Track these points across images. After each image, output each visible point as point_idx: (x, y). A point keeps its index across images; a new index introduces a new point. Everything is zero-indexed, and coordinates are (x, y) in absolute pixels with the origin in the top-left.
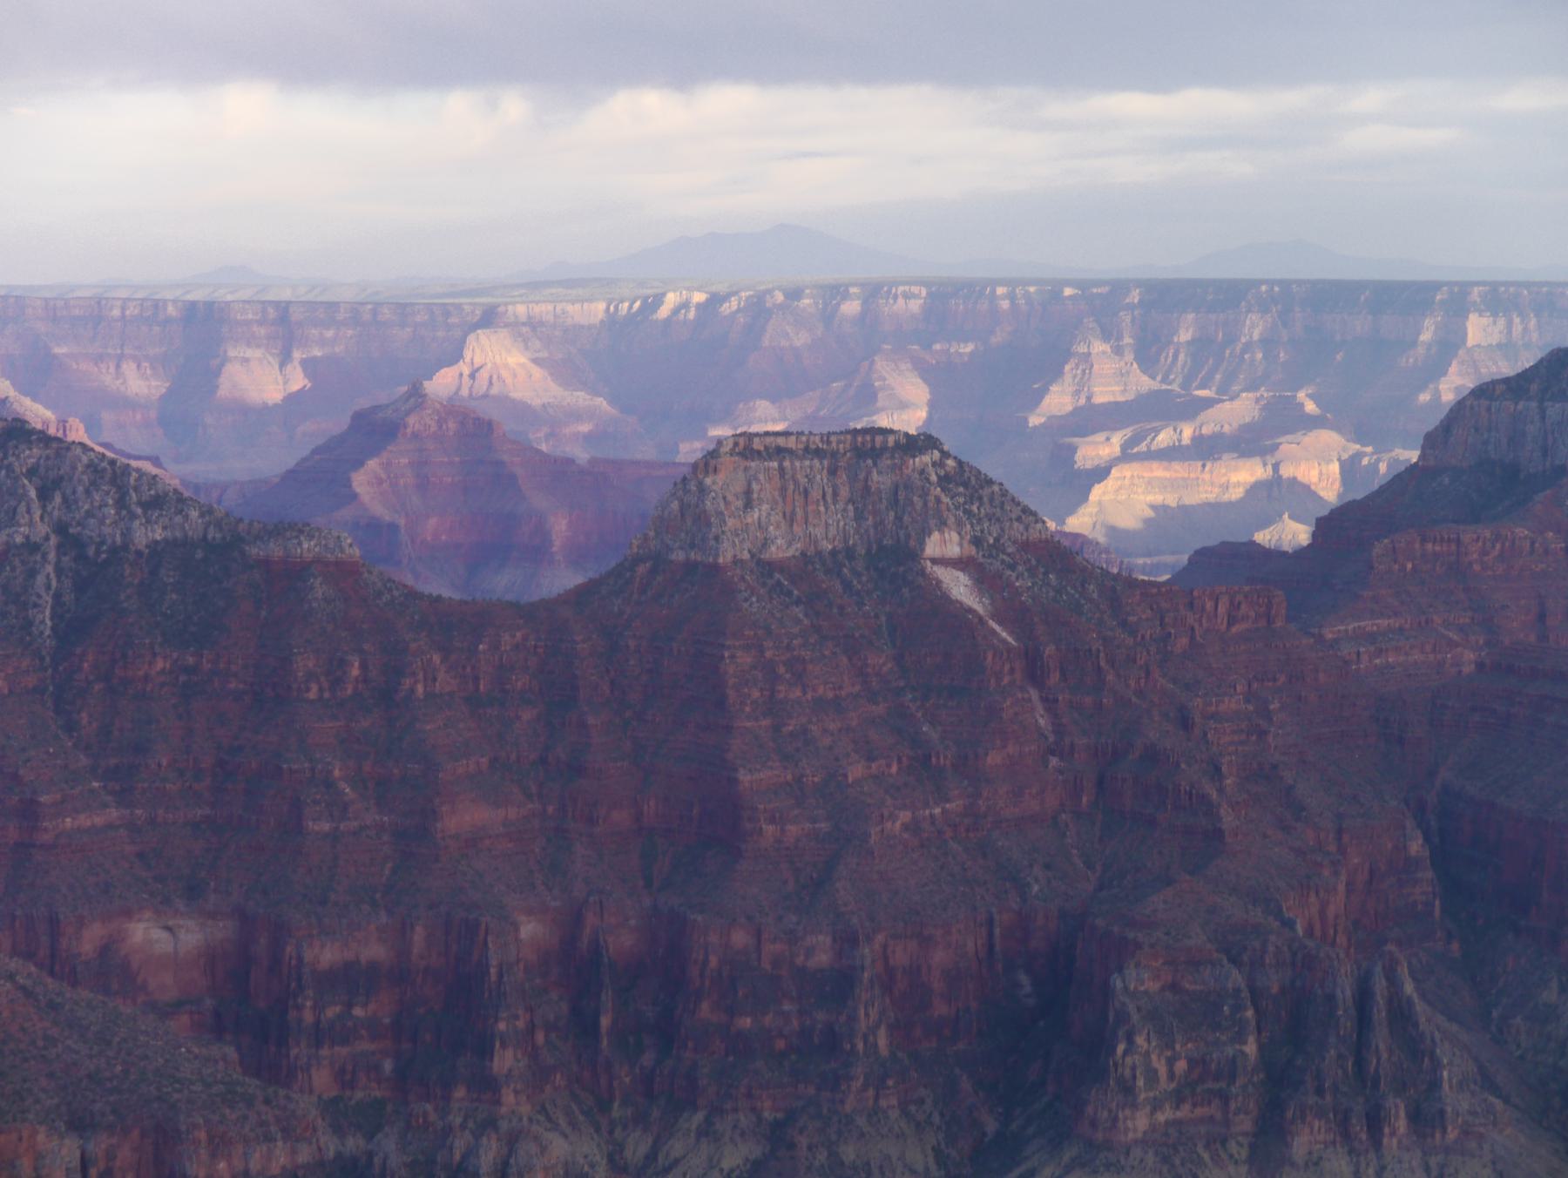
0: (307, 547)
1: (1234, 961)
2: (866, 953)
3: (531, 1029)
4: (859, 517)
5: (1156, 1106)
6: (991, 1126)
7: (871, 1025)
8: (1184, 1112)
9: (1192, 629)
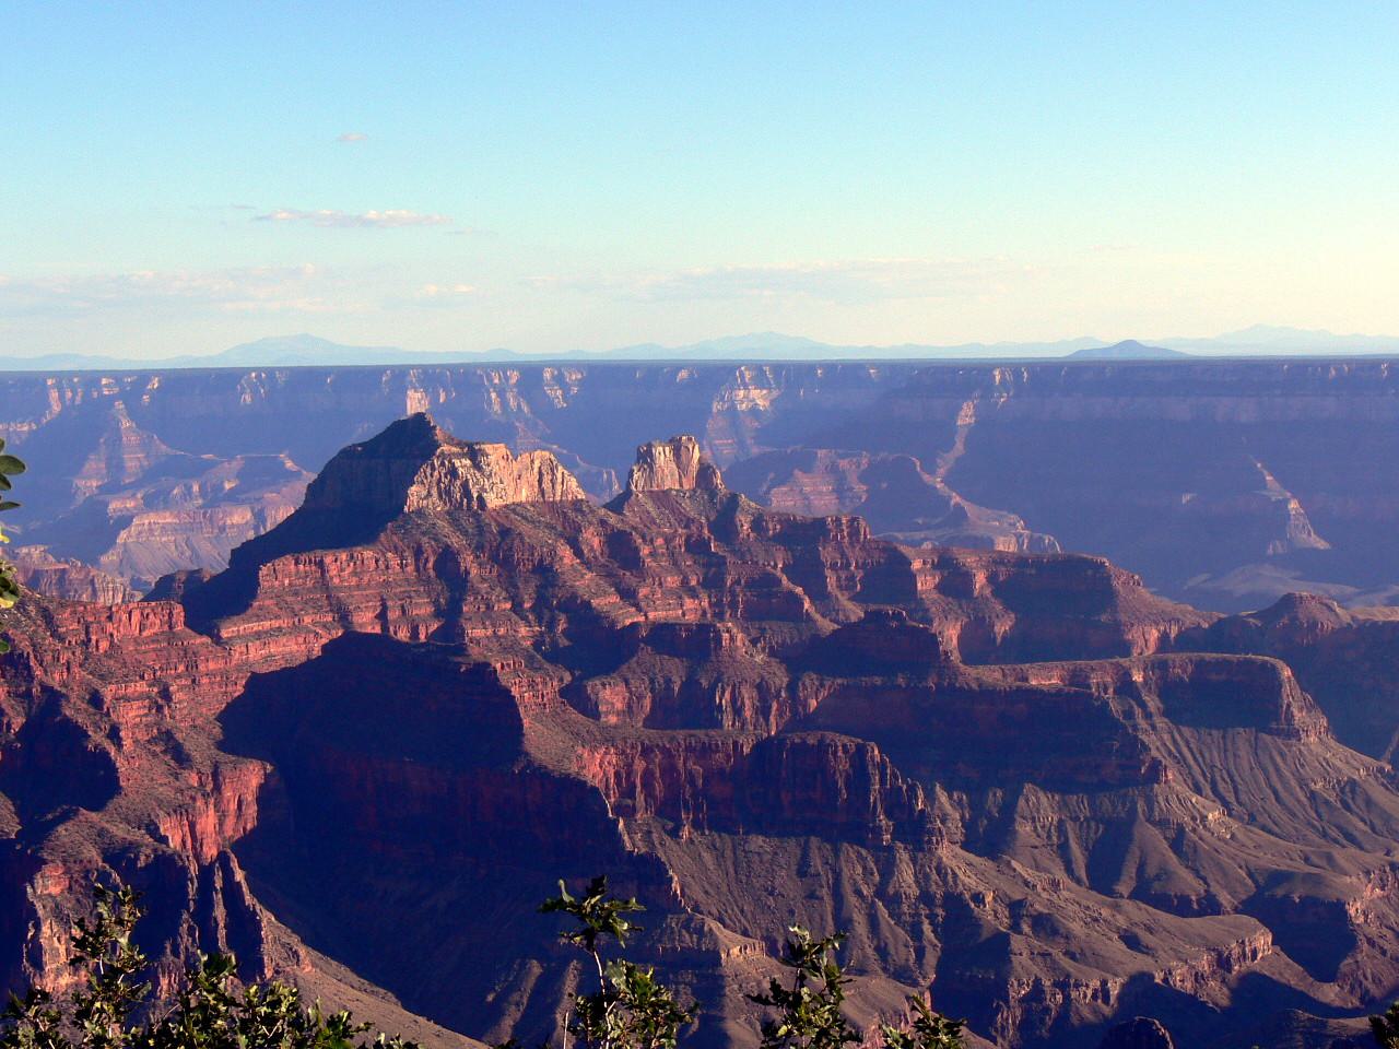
5: (58, 974)
9: (112, 635)
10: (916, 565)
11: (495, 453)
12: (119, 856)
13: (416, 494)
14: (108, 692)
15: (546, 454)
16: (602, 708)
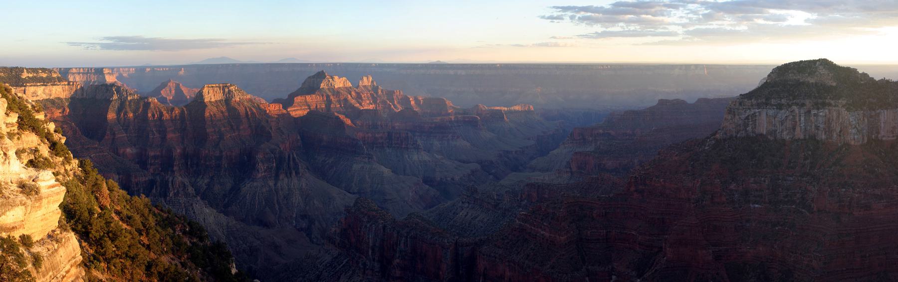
11: (336, 78)
13: (322, 85)
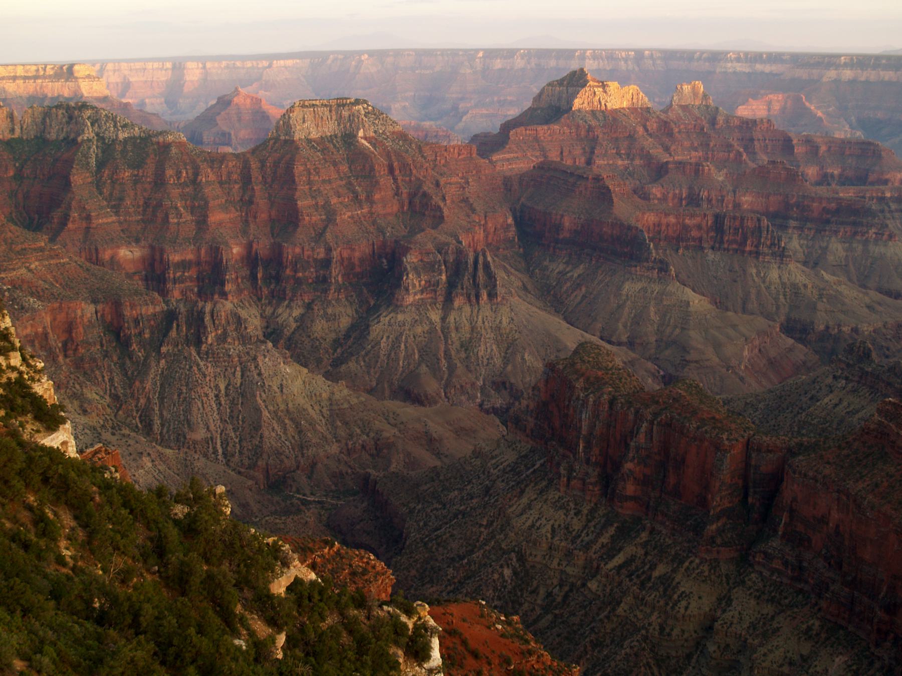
0: (170, 138)
1: (440, 253)
2: (335, 254)
3: (237, 278)
4: (339, 125)
5: (415, 294)
6: (372, 303)
7: (336, 274)
8: (424, 296)
10: (795, 142)
11: (613, 86)
12: (441, 248)
13: (577, 103)
14: (442, 181)
15: (635, 87)
16: (651, 197)
